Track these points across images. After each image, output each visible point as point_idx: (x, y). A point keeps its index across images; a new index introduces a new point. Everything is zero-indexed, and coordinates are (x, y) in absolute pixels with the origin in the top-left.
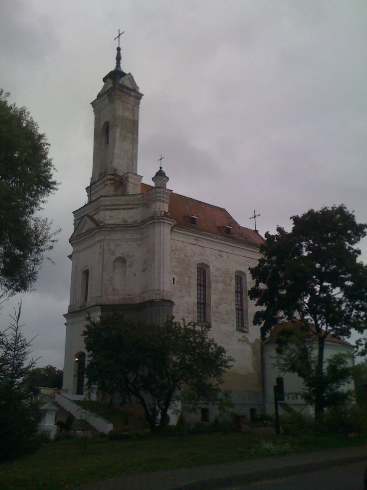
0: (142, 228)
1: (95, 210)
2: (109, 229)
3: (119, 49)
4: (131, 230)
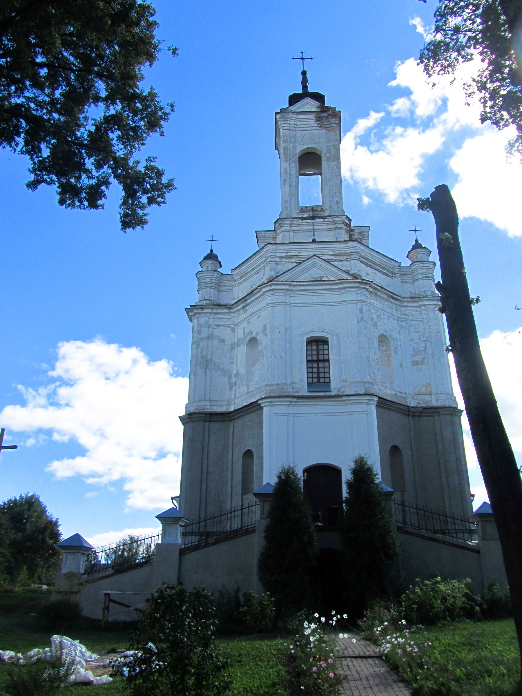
0: (406, 306)
1: (335, 255)
2: (371, 290)
3: (304, 73)
4: (392, 302)
